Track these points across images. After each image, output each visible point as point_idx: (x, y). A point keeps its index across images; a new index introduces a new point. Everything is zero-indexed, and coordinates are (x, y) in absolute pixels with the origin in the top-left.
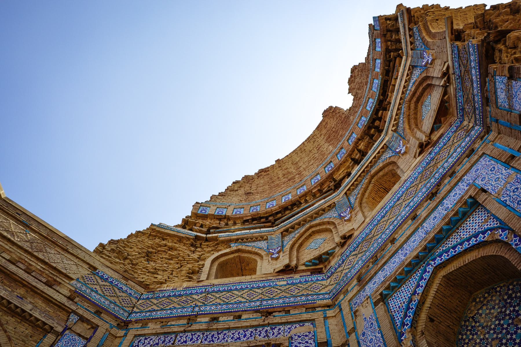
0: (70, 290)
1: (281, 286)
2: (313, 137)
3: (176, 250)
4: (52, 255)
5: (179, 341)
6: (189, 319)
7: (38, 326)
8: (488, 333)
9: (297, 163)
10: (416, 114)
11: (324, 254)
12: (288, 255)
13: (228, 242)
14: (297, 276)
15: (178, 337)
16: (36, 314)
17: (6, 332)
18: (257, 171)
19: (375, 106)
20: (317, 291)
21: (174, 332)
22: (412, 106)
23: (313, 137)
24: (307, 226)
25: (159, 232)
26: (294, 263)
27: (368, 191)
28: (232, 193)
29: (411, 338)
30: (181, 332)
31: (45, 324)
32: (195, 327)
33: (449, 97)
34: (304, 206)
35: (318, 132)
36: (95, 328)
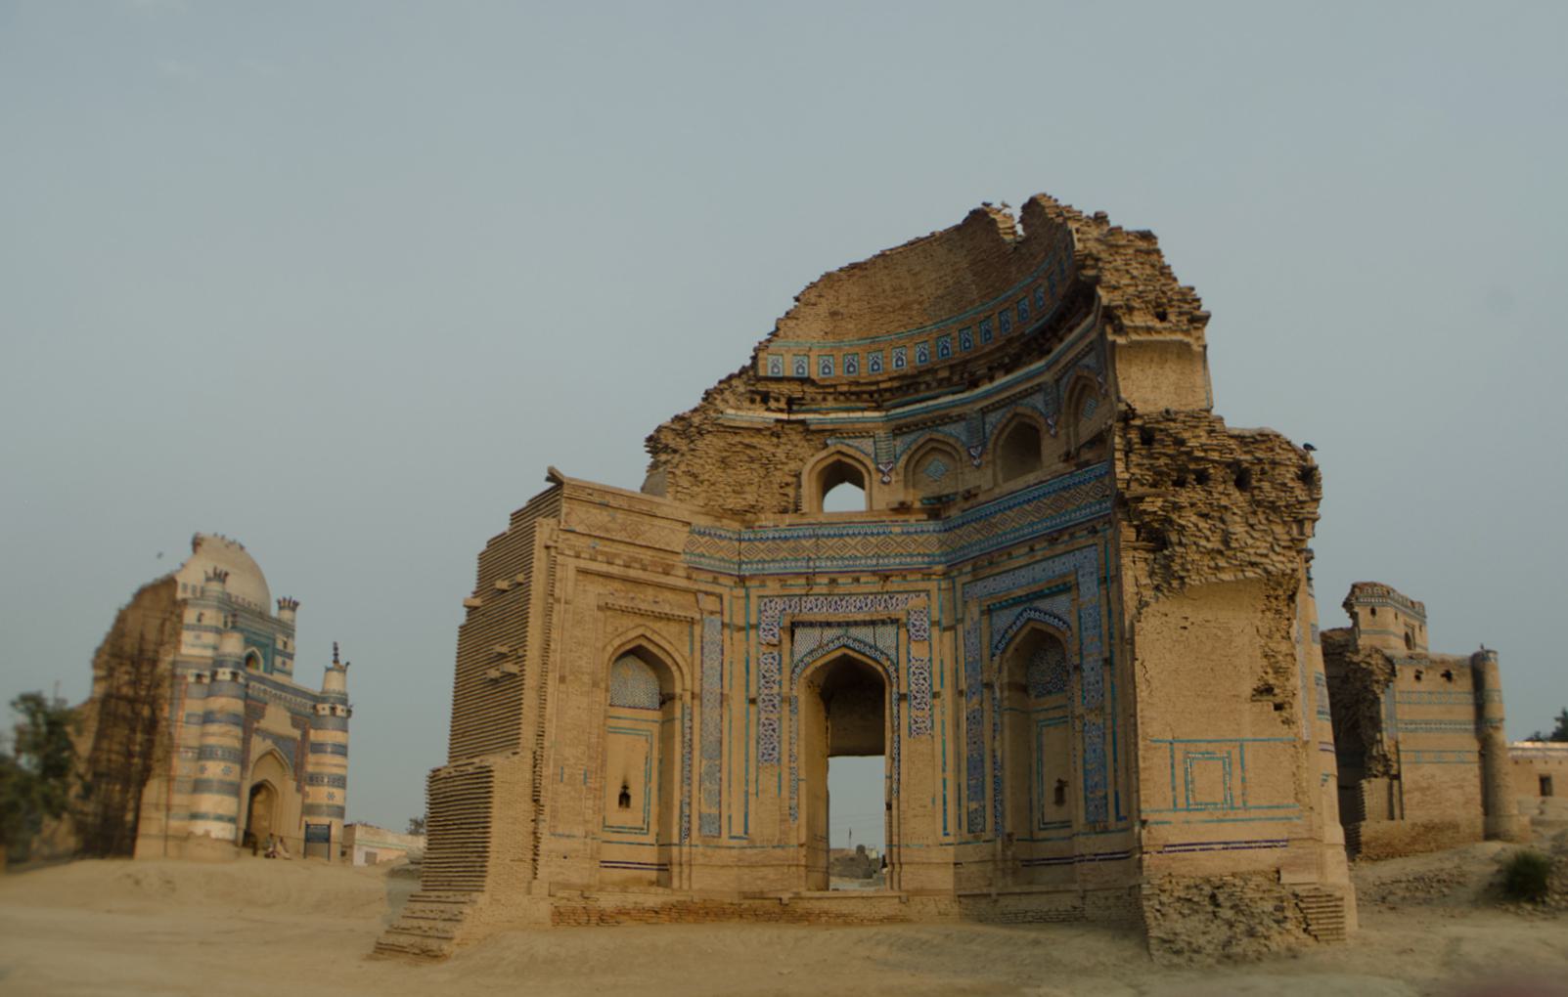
14: (912, 519)
16: (677, 612)
28: (807, 309)
36: (720, 597)
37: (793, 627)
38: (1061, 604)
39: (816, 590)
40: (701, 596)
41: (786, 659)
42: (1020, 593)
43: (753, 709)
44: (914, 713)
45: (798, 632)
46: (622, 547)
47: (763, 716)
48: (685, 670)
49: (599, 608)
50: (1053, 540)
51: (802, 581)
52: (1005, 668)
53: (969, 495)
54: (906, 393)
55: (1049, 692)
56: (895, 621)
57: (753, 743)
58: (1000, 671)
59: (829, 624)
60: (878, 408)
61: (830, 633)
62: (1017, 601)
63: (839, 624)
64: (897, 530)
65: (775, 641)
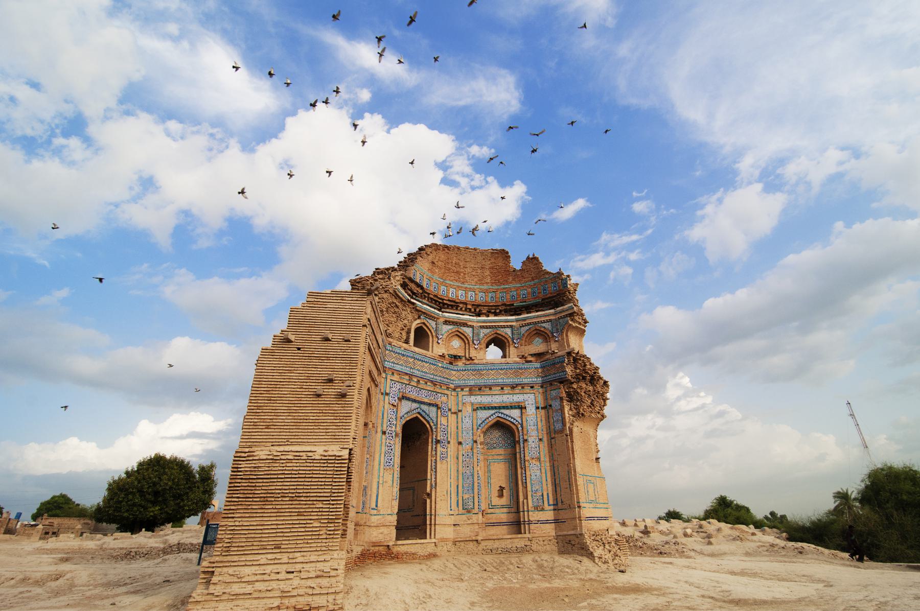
39: (412, 383)
43: (384, 437)
50: (513, 387)
54: (452, 308)
57: (383, 455)
59: (414, 401)
60: (439, 310)
62: (495, 408)
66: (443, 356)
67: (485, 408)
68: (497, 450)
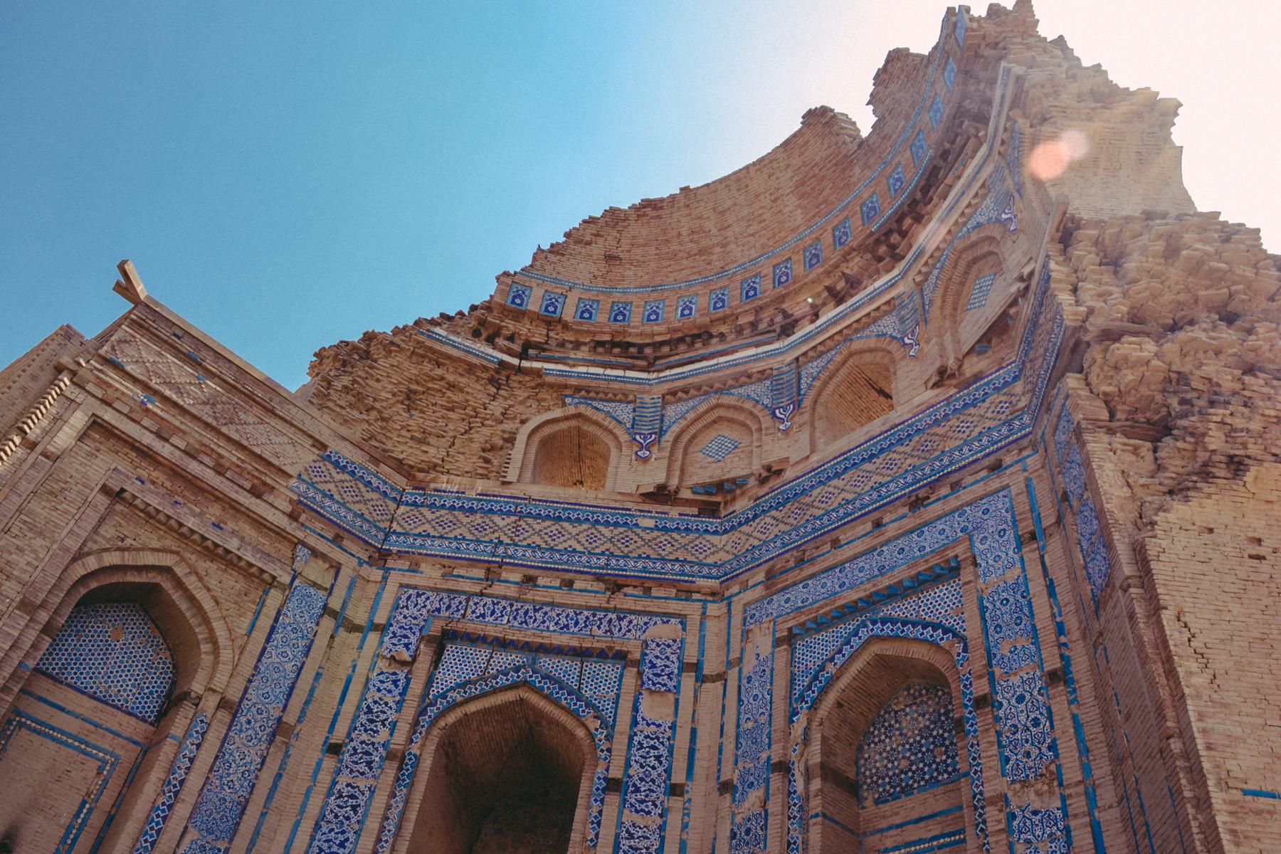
0: (291, 501)
1: (645, 529)
2: (771, 161)
3: (461, 390)
4: (251, 428)
5: (473, 612)
6: (488, 569)
7: (252, 575)
8: (903, 745)
9: (722, 213)
10: (962, 284)
11: (728, 480)
12: (666, 461)
13: (561, 390)
14: (674, 512)
15: (471, 603)
16: (248, 556)
17: (209, 590)
18: (637, 201)
19: (903, 204)
20: (701, 557)
21: (464, 593)
22: (962, 264)
23: (771, 161)
24: (713, 401)
25: (430, 349)
26: (674, 482)
27: (836, 380)
28: (578, 248)
29: (805, 725)
30: (476, 594)
31: (262, 571)
32: (498, 589)
33: (1017, 313)
34: (716, 345)
35: (784, 155)
36: (337, 568)
37: (441, 642)
38: (938, 603)
40: (302, 552)
41: (416, 687)
42: (854, 596)
43: (329, 763)
44: (629, 817)
45: (451, 650)
46: (195, 427)
47: (343, 780)
48: (226, 655)
49: (105, 490)
51: (479, 573)
52: (816, 737)
53: (772, 472)
55: (907, 791)
56: (621, 656)
57: (307, 827)
58: (806, 741)
59: (503, 644)
61: (505, 659)
62: (851, 610)
63: (526, 647)
64: (650, 523)
65: (406, 656)
66: (661, 495)
67: (820, 625)
68: (917, 797)
